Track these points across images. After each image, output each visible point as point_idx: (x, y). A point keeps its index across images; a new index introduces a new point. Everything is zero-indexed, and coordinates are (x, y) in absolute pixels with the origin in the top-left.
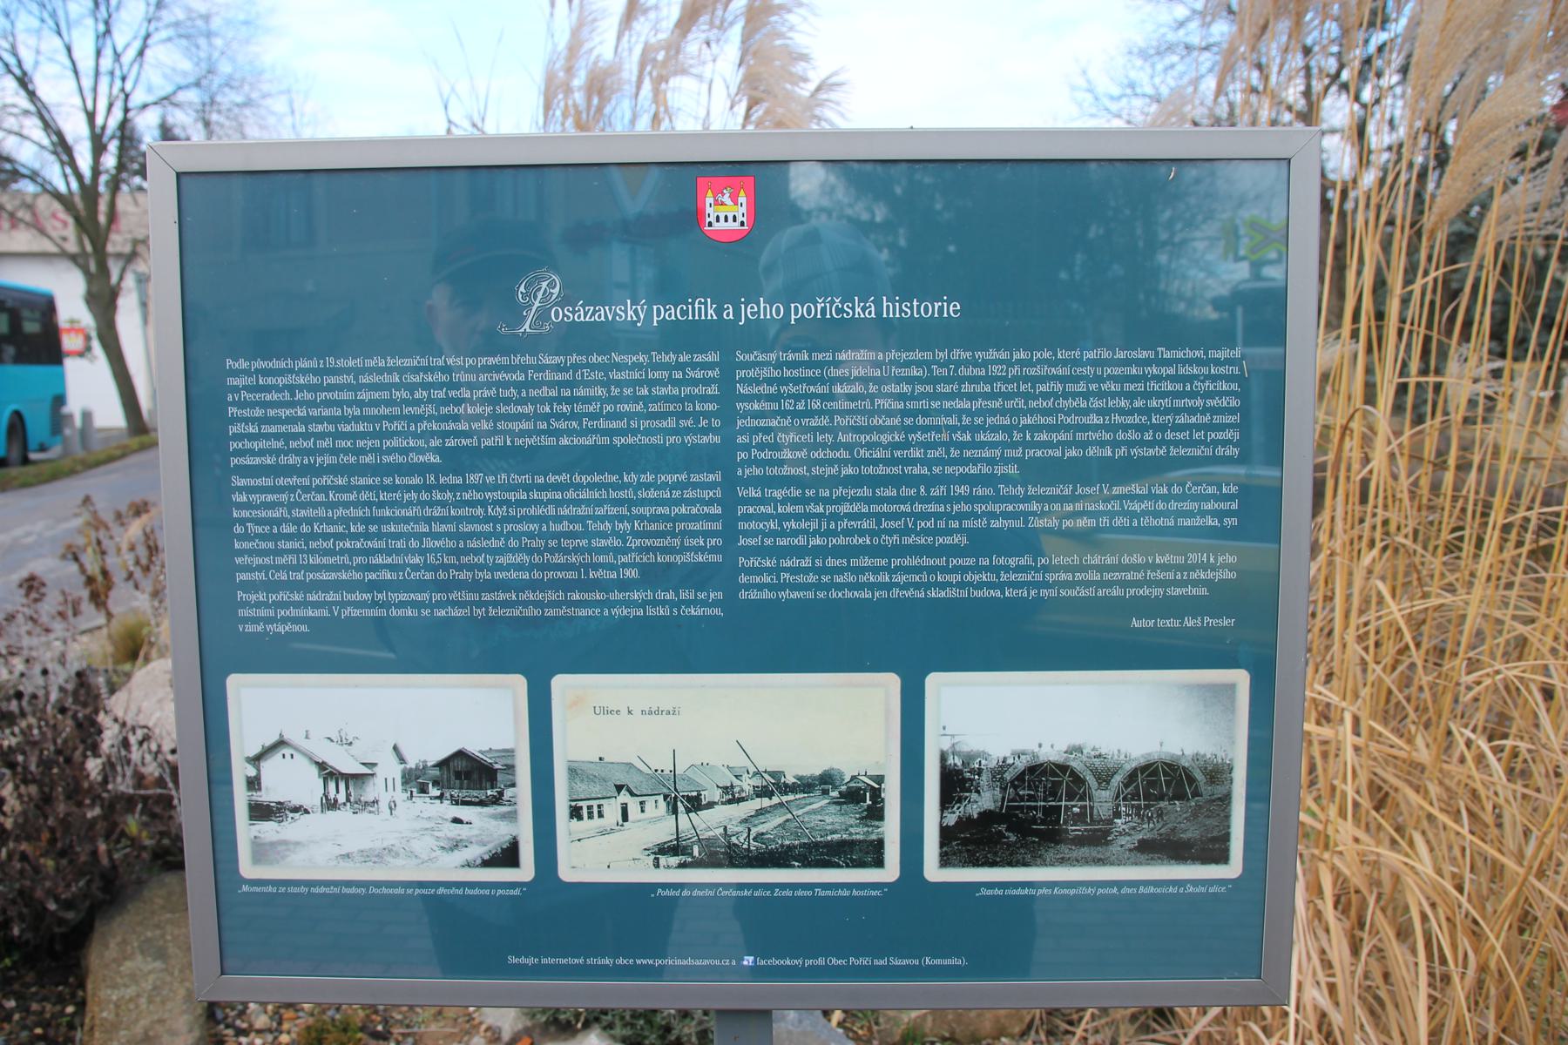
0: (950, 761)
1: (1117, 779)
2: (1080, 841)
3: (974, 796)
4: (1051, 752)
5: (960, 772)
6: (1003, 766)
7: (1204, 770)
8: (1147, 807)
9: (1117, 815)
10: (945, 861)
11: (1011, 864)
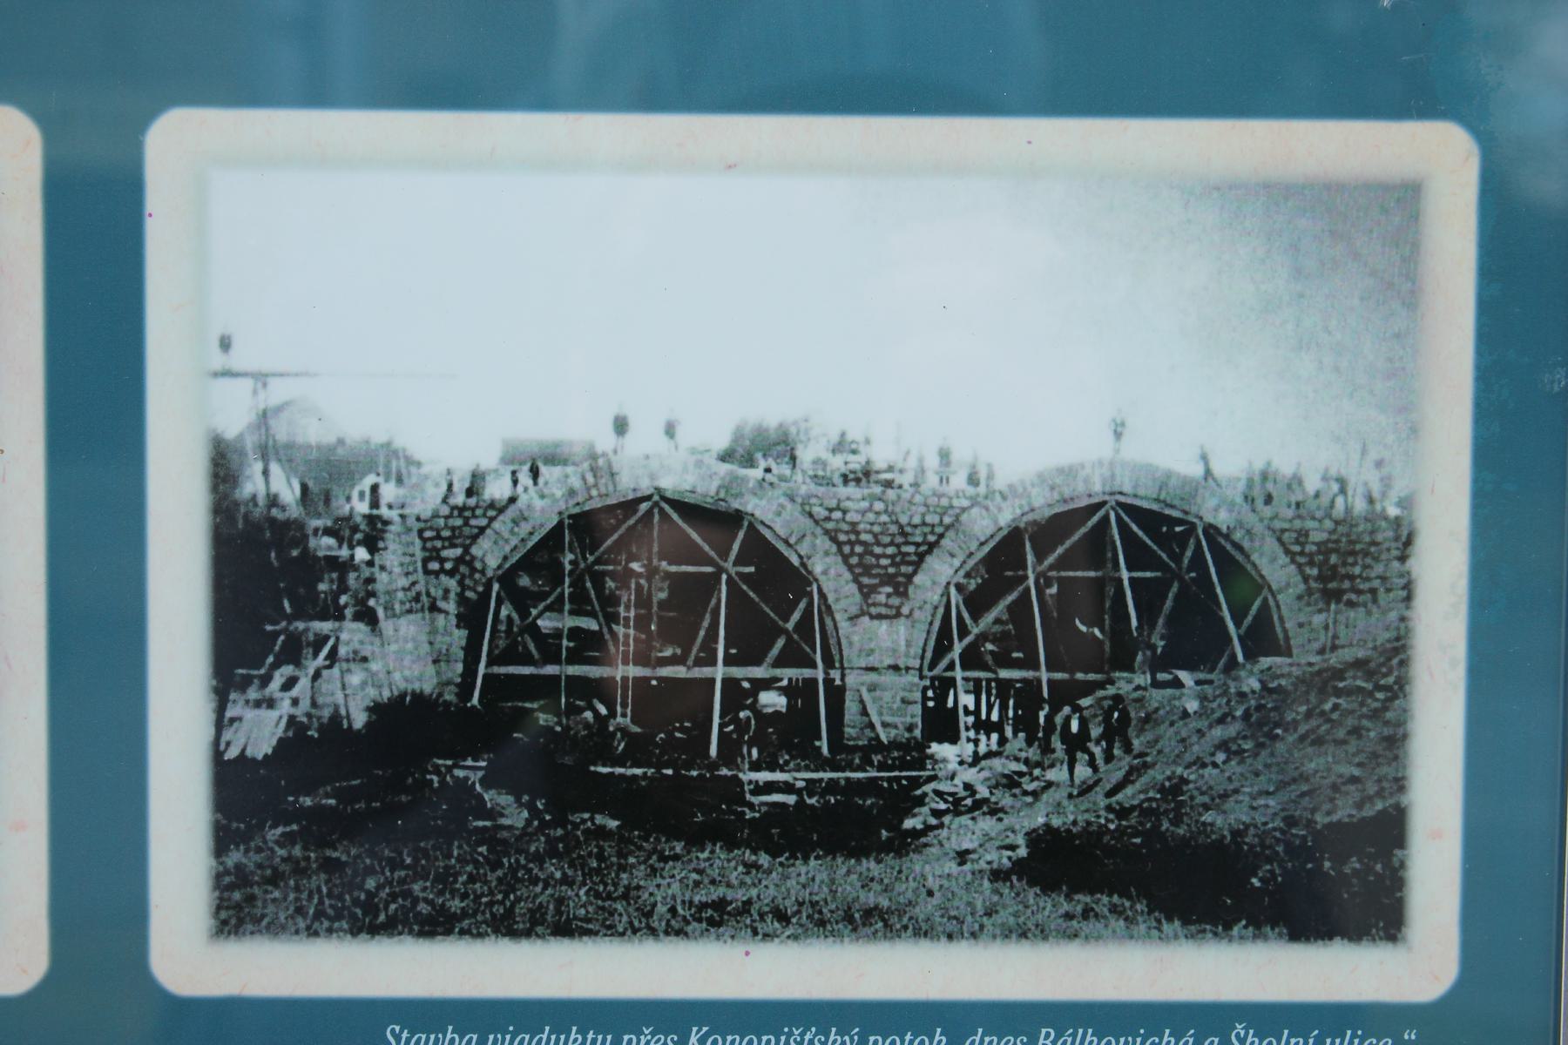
0: (252, 485)
1: (940, 575)
2: (790, 834)
3: (352, 634)
4: (669, 442)
5: (287, 533)
6: (468, 513)
7: (1294, 545)
8: (1064, 695)
9: (942, 724)
10: (238, 910)
11: (507, 926)
